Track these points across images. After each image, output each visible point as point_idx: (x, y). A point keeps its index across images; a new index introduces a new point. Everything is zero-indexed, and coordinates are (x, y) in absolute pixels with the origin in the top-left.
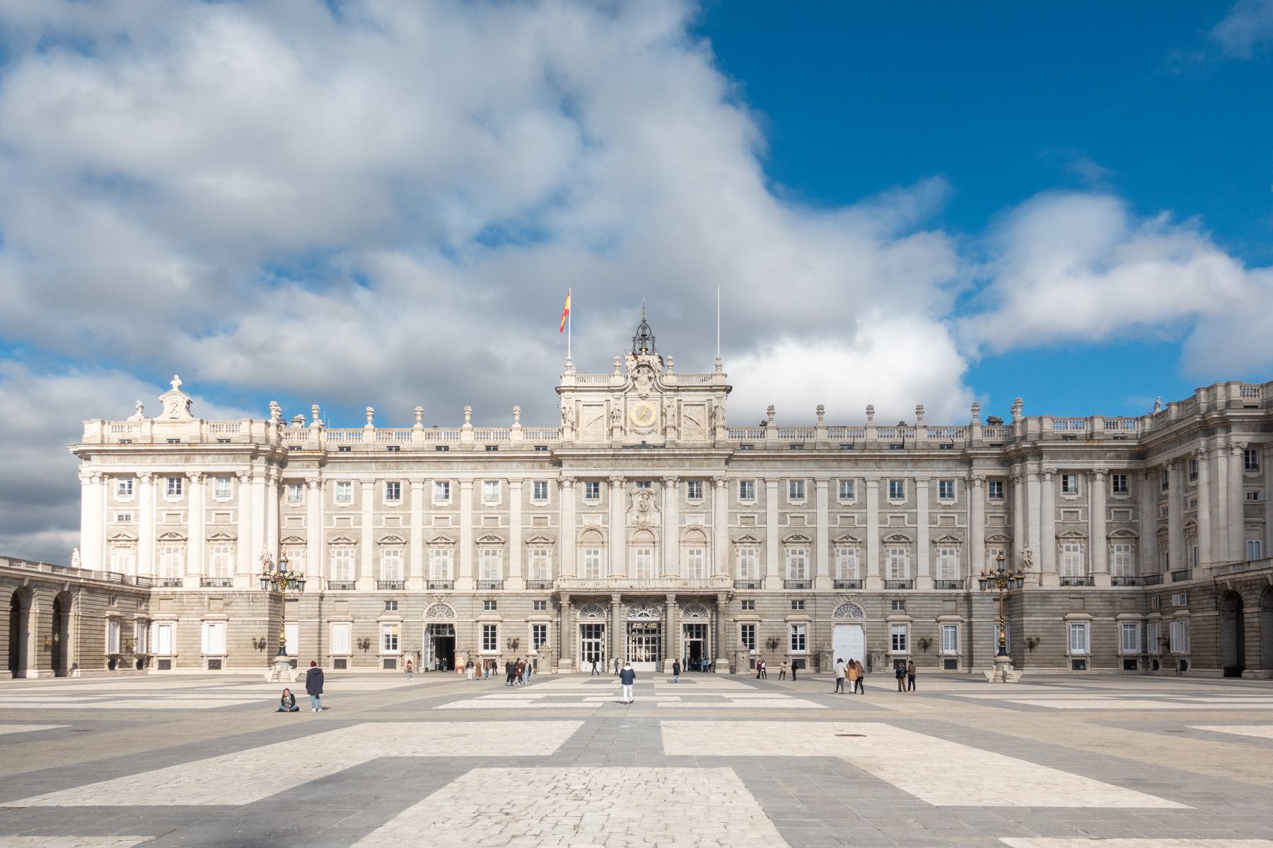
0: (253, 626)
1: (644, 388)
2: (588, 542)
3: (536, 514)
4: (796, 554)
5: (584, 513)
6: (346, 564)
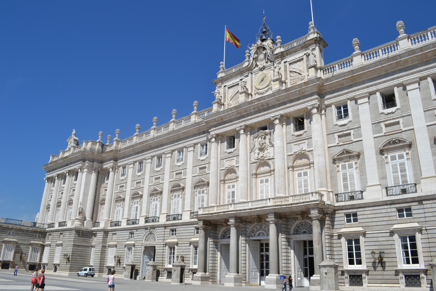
0: (68, 248)
1: (262, 63)
2: (229, 180)
3: (201, 165)
4: (395, 159)
5: (226, 159)
6: (120, 211)
